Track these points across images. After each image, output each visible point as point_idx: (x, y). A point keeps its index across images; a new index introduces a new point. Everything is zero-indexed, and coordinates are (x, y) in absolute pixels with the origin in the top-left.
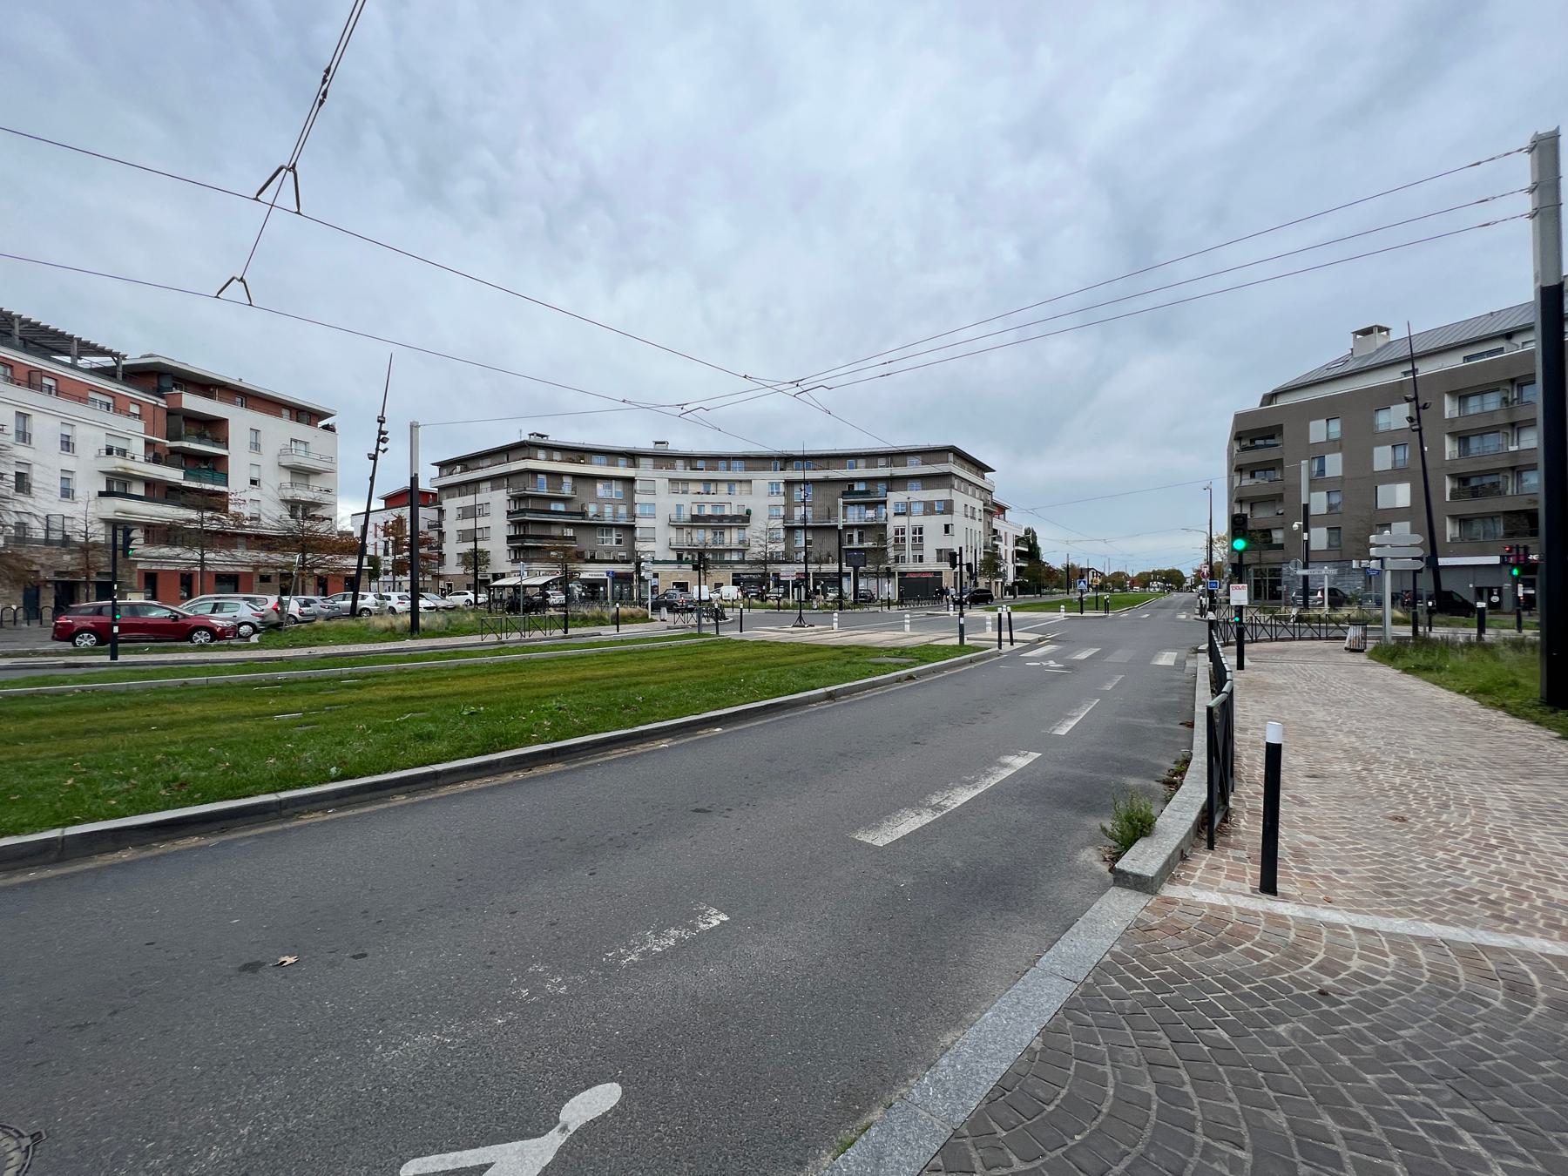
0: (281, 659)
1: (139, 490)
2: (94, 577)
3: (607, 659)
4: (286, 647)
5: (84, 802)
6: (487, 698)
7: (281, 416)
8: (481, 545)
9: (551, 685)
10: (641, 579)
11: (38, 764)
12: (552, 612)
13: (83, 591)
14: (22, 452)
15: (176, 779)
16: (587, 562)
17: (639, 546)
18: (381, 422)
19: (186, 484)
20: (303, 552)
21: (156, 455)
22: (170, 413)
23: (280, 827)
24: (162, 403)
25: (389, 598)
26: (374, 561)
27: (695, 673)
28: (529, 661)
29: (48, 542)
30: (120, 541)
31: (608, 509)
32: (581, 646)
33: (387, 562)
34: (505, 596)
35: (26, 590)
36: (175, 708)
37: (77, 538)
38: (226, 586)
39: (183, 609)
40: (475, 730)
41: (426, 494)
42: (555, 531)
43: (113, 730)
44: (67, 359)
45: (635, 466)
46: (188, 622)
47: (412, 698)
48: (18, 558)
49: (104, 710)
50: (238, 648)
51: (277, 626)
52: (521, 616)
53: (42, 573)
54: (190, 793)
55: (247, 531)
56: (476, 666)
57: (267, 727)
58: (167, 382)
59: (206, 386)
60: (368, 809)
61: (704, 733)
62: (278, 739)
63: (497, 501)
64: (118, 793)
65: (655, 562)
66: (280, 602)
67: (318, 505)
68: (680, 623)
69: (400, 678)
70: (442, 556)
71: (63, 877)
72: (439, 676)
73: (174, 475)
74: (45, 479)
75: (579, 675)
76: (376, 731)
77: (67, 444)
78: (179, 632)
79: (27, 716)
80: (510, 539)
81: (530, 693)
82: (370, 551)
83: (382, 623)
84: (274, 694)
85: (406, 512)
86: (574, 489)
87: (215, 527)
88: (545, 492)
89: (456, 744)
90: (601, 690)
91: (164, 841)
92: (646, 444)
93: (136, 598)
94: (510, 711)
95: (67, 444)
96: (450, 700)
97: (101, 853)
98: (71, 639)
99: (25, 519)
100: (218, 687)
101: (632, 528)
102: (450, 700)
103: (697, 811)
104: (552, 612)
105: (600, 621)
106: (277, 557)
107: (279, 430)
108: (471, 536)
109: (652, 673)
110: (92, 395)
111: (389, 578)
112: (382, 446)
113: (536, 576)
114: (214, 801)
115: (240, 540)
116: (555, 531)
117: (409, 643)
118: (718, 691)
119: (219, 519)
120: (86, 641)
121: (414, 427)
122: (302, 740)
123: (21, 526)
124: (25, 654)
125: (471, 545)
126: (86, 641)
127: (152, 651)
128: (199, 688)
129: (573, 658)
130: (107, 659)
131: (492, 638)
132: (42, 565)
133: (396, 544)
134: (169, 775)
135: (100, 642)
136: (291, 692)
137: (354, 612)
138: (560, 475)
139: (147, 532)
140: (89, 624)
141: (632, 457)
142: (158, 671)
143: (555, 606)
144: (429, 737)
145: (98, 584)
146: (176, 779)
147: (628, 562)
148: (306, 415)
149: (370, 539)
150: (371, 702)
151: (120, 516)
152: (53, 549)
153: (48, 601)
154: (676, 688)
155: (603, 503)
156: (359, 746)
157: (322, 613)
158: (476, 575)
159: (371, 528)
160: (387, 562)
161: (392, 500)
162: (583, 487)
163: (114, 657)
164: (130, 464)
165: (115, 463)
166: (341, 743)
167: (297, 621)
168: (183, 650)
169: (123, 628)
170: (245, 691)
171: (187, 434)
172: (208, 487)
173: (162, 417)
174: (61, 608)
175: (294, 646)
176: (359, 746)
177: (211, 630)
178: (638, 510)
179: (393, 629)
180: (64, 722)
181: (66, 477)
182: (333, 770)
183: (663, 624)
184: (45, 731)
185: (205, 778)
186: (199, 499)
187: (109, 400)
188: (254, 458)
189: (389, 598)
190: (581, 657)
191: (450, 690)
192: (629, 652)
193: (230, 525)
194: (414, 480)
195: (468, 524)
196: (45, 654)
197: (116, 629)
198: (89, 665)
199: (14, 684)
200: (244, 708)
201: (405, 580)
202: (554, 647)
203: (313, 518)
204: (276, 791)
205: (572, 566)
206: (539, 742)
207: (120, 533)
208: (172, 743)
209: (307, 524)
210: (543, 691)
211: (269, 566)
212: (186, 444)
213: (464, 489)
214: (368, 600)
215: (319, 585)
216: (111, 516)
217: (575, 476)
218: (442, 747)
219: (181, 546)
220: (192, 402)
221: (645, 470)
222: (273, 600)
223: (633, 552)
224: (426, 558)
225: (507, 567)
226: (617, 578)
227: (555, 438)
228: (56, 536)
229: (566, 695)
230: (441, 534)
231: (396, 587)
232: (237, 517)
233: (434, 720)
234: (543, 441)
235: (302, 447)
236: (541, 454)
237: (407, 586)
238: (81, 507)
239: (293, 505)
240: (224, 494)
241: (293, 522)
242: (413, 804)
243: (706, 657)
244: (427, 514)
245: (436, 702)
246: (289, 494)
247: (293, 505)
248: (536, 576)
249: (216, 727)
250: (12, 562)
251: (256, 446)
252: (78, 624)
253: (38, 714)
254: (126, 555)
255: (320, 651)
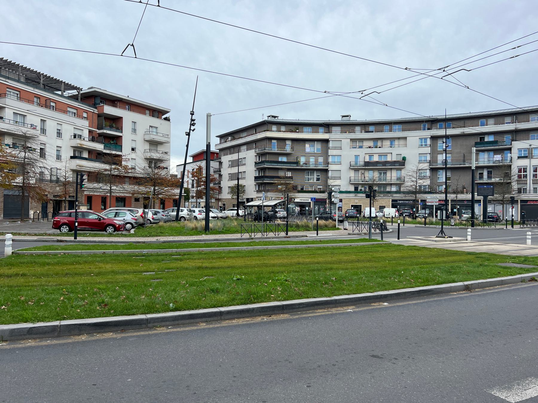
0: (144, 242)
1: (85, 155)
2: (68, 199)
3: (312, 252)
4: (146, 236)
5: (67, 309)
6: (245, 271)
7: (145, 114)
8: (241, 182)
9: (280, 265)
10: (332, 203)
11: (50, 288)
12: (279, 222)
13: (63, 205)
14: (42, 138)
15: (103, 302)
16: (299, 192)
17: (331, 182)
18: (192, 114)
19: (105, 151)
20: (154, 186)
21: (93, 137)
22: (99, 116)
23: (147, 333)
24: (96, 111)
25: (194, 212)
26: (187, 191)
27: (368, 264)
28: (267, 251)
29: (51, 181)
30: (79, 181)
31: (312, 160)
32: (297, 243)
33: (193, 193)
34: (253, 212)
35: (42, 204)
36: (101, 265)
37: (62, 179)
38: (120, 203)
39: (103, 214)
40: (241, 289)
41: (213, 153)
42: (281, 174)
43: (76, 274)
44: (60, 93)
45: (329, 132)
46: (105, 221)
47: (206, 268)
48: (40, 188)
49: (72, 264)
50: (125, 236)
51: (142, 225)
52: (262, 223)
53: (48, 196)
54: (109, 310)
55: (130, 175)
56: (239, 252)
57: (140, 278)
58: (98, 101)
59: (114, 101)
60: (187, 329)
61: (376, 305)
62: (145, 285)
63: (250, 156)
64: (80, 306)
65: (341, 192)
66: (144, 212)
67: (161, 161)
68: (356, 232)
69: (201, 256)
70: (220, 188)
71: (60, 345)
72: (220, 257)
73: (99, 147)
74: (51, 152)
75: (296, 260)
76: (192, 285)
77: (59, 134)
78: (100, 226)
79: (44, 264)
80: (256, 178)
81: (269, 269)
82: (185, 185)
83: (191, 225)
84: (142, 261)
85: (203, 164)
86: (292, 148)
87: (116, 173)
88: (276, 150)
89: (232, 297)
90: (309, 271)
91: (98, 333)
92: (336, 118)
93: (84, 209)
94: (259, 279)
95: (59, 134)
96: (226, 271)
97: (74, 335)
98: (59, 228)
99: (43, 170)
100: (118, 256)
101: (326, 171)
102: (226, 271)
103: (373, 356)
104: (279, 222)
105: (307, 228)
106: (142, 189)
107: (145, 121)
108: (236, 177)
109: (340, 262)
110: (69, 109)
111: (194, 200)
112: (192, 128)
113: (270, 200)
114: (119, 315)
115: (127, 180)
116: (281, 174)
117: (204, 237)
118: (385, 277)
119: (118, 169)
120: (65, 229)
121: (209, 116)
122: (156, 287)
123: (42, 173)
124: (42, 235)
125: (236, 182)
126: (65, 229)
127: (91, 235)
128: (110, 256)
129: (292, 250)
130: (72, 238)
131: (246, 236)
132: (49, 192)
133: (198, 182)
134: (100, 300)
135: (70, 230)
136: (150, 260)
137: (178, 218)
138: (284, 140)
139: (88, 176)
140: (66, 221)
141: (327, 126)
142: (93, 246)
143: (280, 218)
144: (216, 291)
145: (69, 201)
146: (103, 302)
147: (323, 192)
148: (157, 113)
149: (186, 179)
150: (187, 269)
151: (78, 168)
152: (53, 184)
153: (50, 210)
154: (357, 274)
155: (309, 156)
156: (183, 293)
157: (162, 219)
158: (238, 198)
159: (186, 173)
160: (193, 193)
161: (197, 157)
162: (297, 147)
163: (75, 238)
164: (83, 142)
165: (77, 142)
166: (174, 290)
167: (151, 223)
168: (103, 236)
169: (80, 224)
170: (129, 259)
171: (106, 126)
172: (114, 152)
173: (96, 117)
174: (55, 214)
175: (150, 236)
176: (183, 293)
177: (114, 225)
178: (330, 160)
179: (196, 228)
180: (58, 268)
181: (59, 149)
182: (171, 305)
183: (346, 231)
184: (51, 273)
185: (115, 303)
186: (110, 158)
187: (75, 111)
188: (133, 137)
189: (194, 212)
190: (296, 250)
191: (226, 264)
192: (324, 248)
193: (123, 172)
194: (208, 146)
195: (234, 170)
196: (50, 235)
197: (77, 224)
198: (66, 241)
199: (39, 248)
200: (129, 268)
201: (202, 201)
202: (281, 243)
203: (159, 168)
204: (145, 314)
205: (291, 195)
206: (275, 300)
207: (79, 177)
208: (100, 283)
209: (156, 171)
210: (276, 269)
211: (139, 193)
212: (105, 131)
213: (232, 150)
214: (184, 213)
215: (161, 203)
216: (75, 168)
217: (294, 140)
218: (223, 297)
219: (102, 183)
220: (109, 110)
221: (335, 135)
222: (141, 211)
223: (326, 185)
224: (213, 189)
225: (254, 195)
226: (317, 201)
227: (285, 117)
228: (54, 178)
229: (289, 272)
230: (220, 176)
231: (198, 205)
232: (126, 168)
233: (219, 281)
234: (276, 120)
235: (154, 130)
236: (274, 128)
237: (203, 204)
238: (64, 164)
239: (151, 161)
240: (120, 156)
241: (150, 170)
242: (209, 329)
243: (375, 255)
244: (214, 165)
245: (219, 271)
246: (148, 155)
247: (151, 161)
248: (270, 200)
249: (118, 277)
250: (38, 190)
251: (134, 131)
252: (62, 221)
253: (48, 264)
254: (81, 187)
255: (162, 239)
